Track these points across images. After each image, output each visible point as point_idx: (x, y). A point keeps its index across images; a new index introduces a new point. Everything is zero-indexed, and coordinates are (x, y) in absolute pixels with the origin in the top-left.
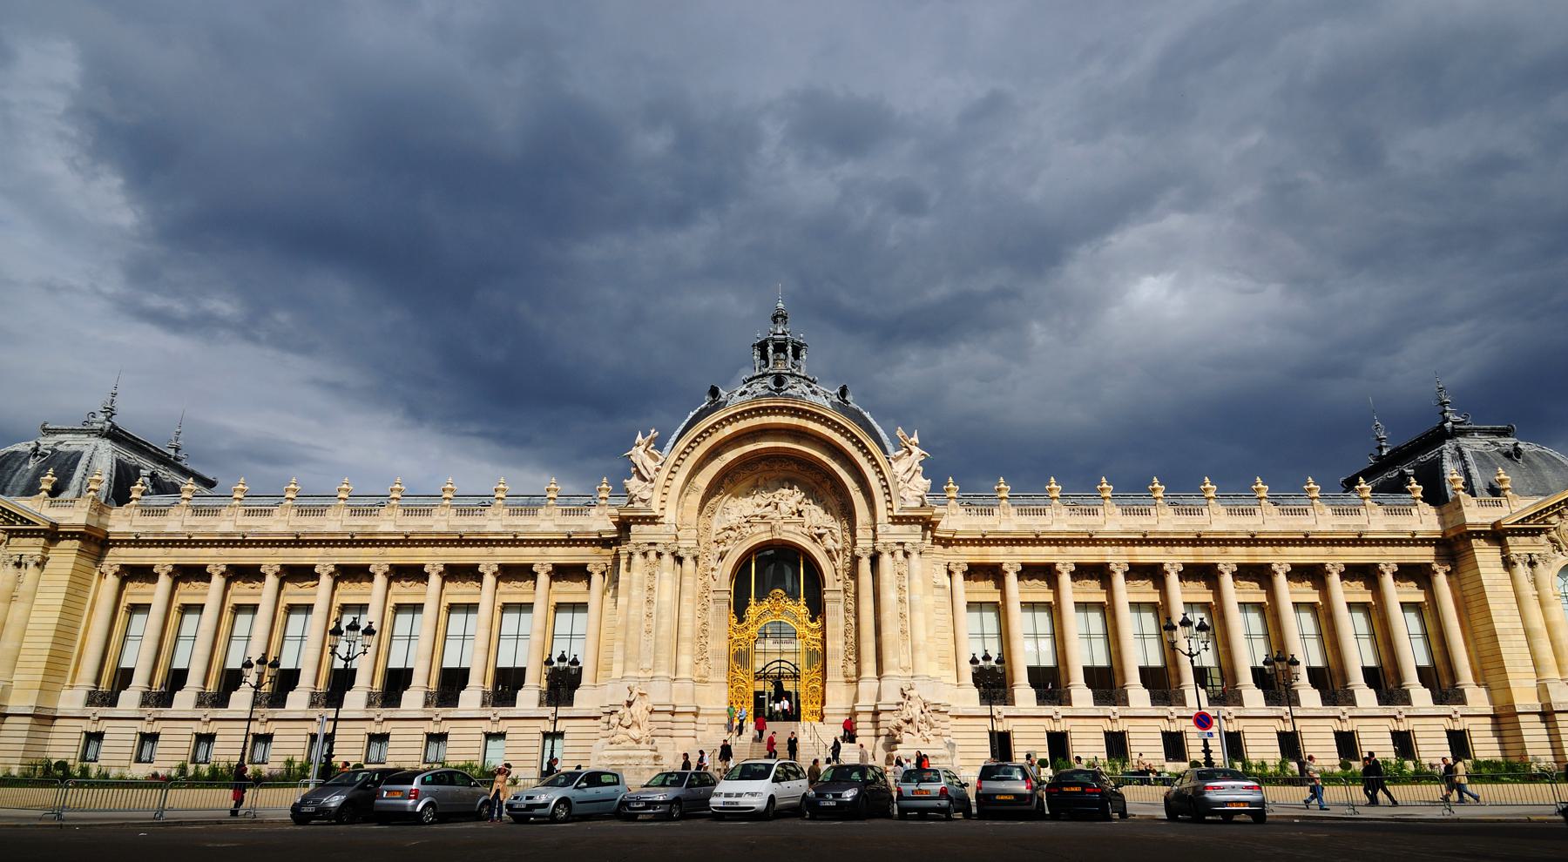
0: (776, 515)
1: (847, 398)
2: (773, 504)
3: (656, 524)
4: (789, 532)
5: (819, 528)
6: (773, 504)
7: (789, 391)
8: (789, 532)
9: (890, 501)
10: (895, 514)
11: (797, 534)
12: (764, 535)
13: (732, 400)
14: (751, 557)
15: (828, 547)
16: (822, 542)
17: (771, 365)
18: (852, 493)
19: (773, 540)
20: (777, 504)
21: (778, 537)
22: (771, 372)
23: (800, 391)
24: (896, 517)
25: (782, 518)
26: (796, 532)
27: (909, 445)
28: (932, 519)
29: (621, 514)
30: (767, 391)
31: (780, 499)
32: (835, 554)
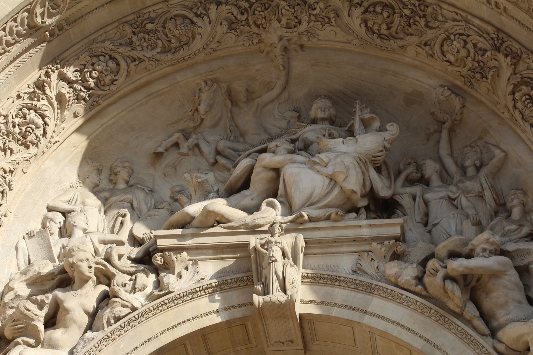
16: (485, 317)
20: (277, 171)
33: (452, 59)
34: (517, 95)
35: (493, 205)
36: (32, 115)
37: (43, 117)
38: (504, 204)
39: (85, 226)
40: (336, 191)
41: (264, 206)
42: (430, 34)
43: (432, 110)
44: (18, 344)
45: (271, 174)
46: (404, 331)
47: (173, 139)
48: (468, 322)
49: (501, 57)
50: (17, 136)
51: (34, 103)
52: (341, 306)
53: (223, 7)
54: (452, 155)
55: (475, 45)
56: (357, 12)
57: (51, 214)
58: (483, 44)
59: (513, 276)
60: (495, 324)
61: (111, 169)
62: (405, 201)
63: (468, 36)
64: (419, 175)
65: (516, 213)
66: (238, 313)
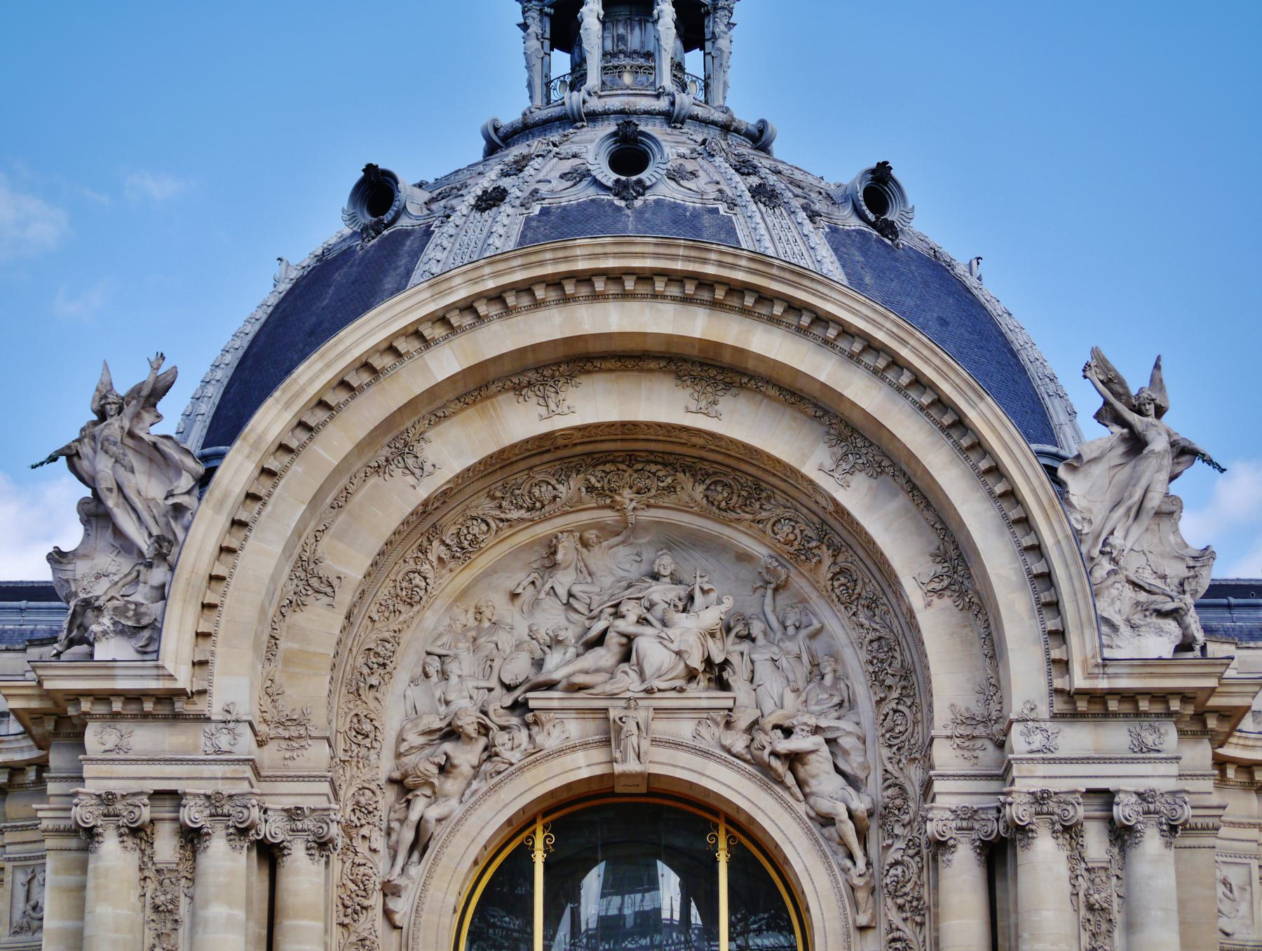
0: (628, 682)
1: (890, 216)
2: (613, 640)
3: (177, 717)
4: (677, 745)
5: (788, 732)
6: (613, 640)
7: (668, 191)
8: (677, 745)
9: (1059, 635)
10: (1079, 681)
11: (706, 754)
12: (580, 758)
13: (449, 228)
14: (534, 832)
15: (825, 806)
16: (801, 784)
17: (594, 78)
18: (915, 596)
19: (611, 776)
20: (630, 638)
21: (632, 766)
22: (595, 104)
23: (712, 192)
24: (1082, 693)
25: (649, 691)
26: (699, 744)
27: (1133, 418)
28: (1214, 702)
29: (48, 685)
30: (583, 193)
31: (643, 621)
32: (849, 829)
33: (782, 540)
34: (836, 584)
35: (809, 667)
36: (418, 580)
37: (425, 578)
38: (818, 665)
39: (460, 673)
40: (682, 666)
41: (619, 675)
42: (764, 515)
43: (760, 570)
44: (417, 795)
45: (624, 640)
46: (735, 794)
47: (530, 579)
48: (788, 788)
49: (824, 548)
50: (405, 598)
51: (418, 567)
52: (683, 768)
53: (581, 476)
54: (774, 611)
55: (802, 531)
56: (701, 488)
57: (429, 659)
58: (808, 532)
59: (825, 749)
60: (807, 790)
61: (476, 608)
62: (735, 659)
63: (797, 522)
64: (746, 633)
65: (828, 679)
66: (598, 771)
